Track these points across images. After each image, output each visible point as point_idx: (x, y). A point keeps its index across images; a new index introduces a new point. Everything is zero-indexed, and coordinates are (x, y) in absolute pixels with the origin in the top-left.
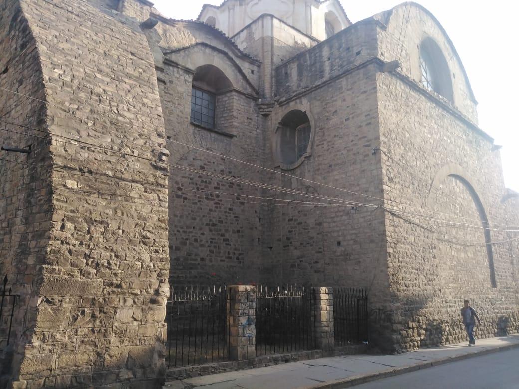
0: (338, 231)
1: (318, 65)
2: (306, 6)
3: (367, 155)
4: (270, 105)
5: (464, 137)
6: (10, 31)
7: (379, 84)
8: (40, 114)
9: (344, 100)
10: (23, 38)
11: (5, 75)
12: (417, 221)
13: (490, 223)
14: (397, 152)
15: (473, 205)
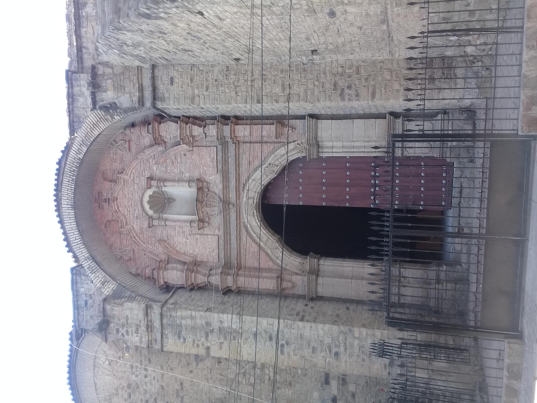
6: (161, 18)
11: (205, 13)
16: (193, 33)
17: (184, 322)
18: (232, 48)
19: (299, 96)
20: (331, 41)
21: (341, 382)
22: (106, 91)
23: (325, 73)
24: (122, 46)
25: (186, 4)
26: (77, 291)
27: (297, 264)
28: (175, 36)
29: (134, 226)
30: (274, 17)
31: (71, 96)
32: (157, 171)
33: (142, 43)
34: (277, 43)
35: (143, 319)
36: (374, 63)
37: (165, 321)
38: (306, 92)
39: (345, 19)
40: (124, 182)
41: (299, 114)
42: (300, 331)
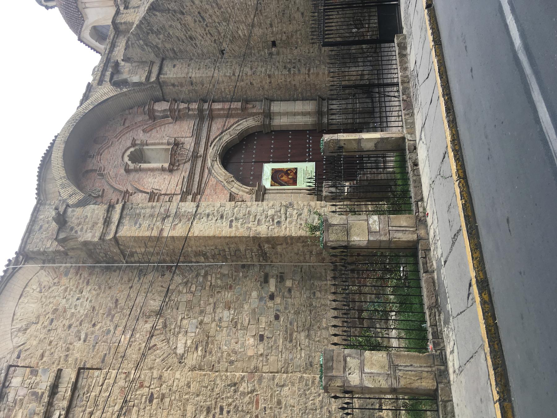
16: (203, 14)
17: (143, 211)
18: (222, 35)
20: (285, 30)
21: (279, 280)
22: (122, 73)
23: (279, 62)
24: (148, 33)
26: (36, 217)
27: (248, 190)
29: (110, 173)
31: (86, 95)
33: (164, 27)
36: (309, 58)
37: (125, 213)
38: (266, 70)
40: (112, 144)
42: (248, 209)
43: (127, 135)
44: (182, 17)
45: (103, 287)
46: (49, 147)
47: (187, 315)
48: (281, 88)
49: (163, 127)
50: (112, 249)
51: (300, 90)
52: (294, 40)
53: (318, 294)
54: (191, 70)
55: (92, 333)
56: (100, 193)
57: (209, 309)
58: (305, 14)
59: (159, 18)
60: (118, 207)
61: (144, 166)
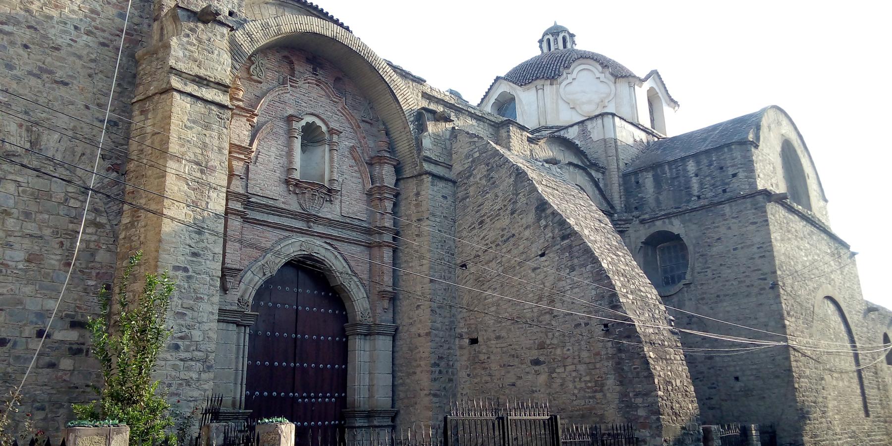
0: (735, 366)
1: (682, 180)
2: (630, 87)
3: (764, 289)
4: (627, 221)
5: (829, 251)
6: (539, 220)
7: (770, 216)
8: (613, 301)
9: (729, 228)
10: (561, 230)
11: (543, 258)
12: (809, 353)
13: (858, 345)
14: (789, 281)
15: (842, 327)
17: (215, 134)
19: (435, 322)
20: (492, 357)
21: (75, 347)
24: (488, 165)
25: (558, 247)
27: (246, 298)
28: (507, 221)
29: (288, 95)
30: (536, 314)
32: (345, 143)
34: (493, 309)
35: (209, 74)
38: (437, 329)
39: (528, 373)
41: (397, 317)
42: (206, 297)
43: (347, 125)
44: (507, 212)
45: (93, 65)
46: (332, 17)
47: (24, 192)
48: (412, 351)
49: (358, 175)
50: (155, 83)
51: (408, 381)
52: (479, 371)
53: (40, 415)
54: (438, 220)
55: (12, 43)
56: (255, 78)
57: (31, 228)
58: (514, 388)
59: (507, 180)
60: (224, 99)
61: (297, 143)
